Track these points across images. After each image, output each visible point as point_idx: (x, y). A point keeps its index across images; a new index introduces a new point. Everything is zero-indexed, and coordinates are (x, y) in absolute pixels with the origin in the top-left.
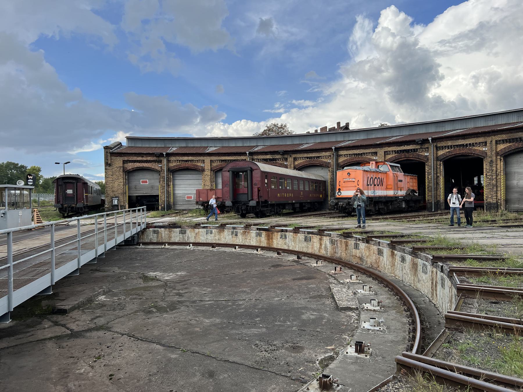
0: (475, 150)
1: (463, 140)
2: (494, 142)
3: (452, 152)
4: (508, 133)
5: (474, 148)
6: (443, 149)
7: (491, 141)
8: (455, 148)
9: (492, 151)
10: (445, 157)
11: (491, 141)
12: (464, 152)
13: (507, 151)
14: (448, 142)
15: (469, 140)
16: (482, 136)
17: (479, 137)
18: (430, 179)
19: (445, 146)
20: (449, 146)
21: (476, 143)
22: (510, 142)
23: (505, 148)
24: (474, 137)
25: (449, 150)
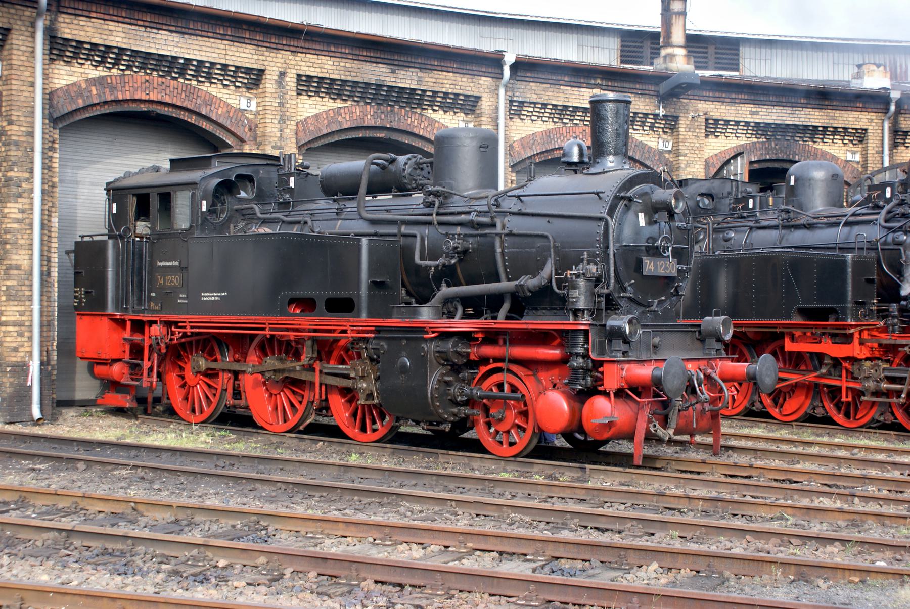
0: (211, 100)
1: (176, 38)
2: (291, 81)
3: (113, 89)
4: (343, 56)
5: (206, 87)
6: (76, 56)
7: (282, 75)
8: (129, 67)
9: (283, 119)
10: (81, 103)
11: (282, 75)
12: (167, 99)
13: (325, 132)
14: (112, 26)
15: (201, 41)
16: (251, 42)
17: (241, 40)
18: (19, 221)
19: (95, 46)
20: (109, 48)
21: (225, 67)
22: (339, 95)
23: (317, 116)
24: (223, 37)
25: (100, 72)
